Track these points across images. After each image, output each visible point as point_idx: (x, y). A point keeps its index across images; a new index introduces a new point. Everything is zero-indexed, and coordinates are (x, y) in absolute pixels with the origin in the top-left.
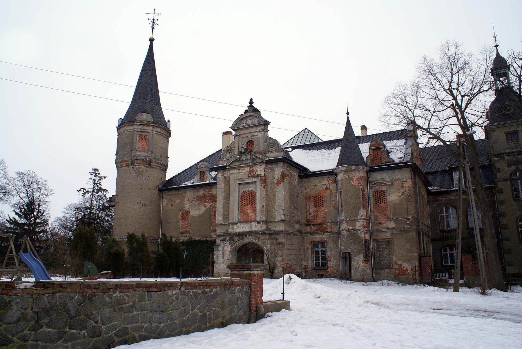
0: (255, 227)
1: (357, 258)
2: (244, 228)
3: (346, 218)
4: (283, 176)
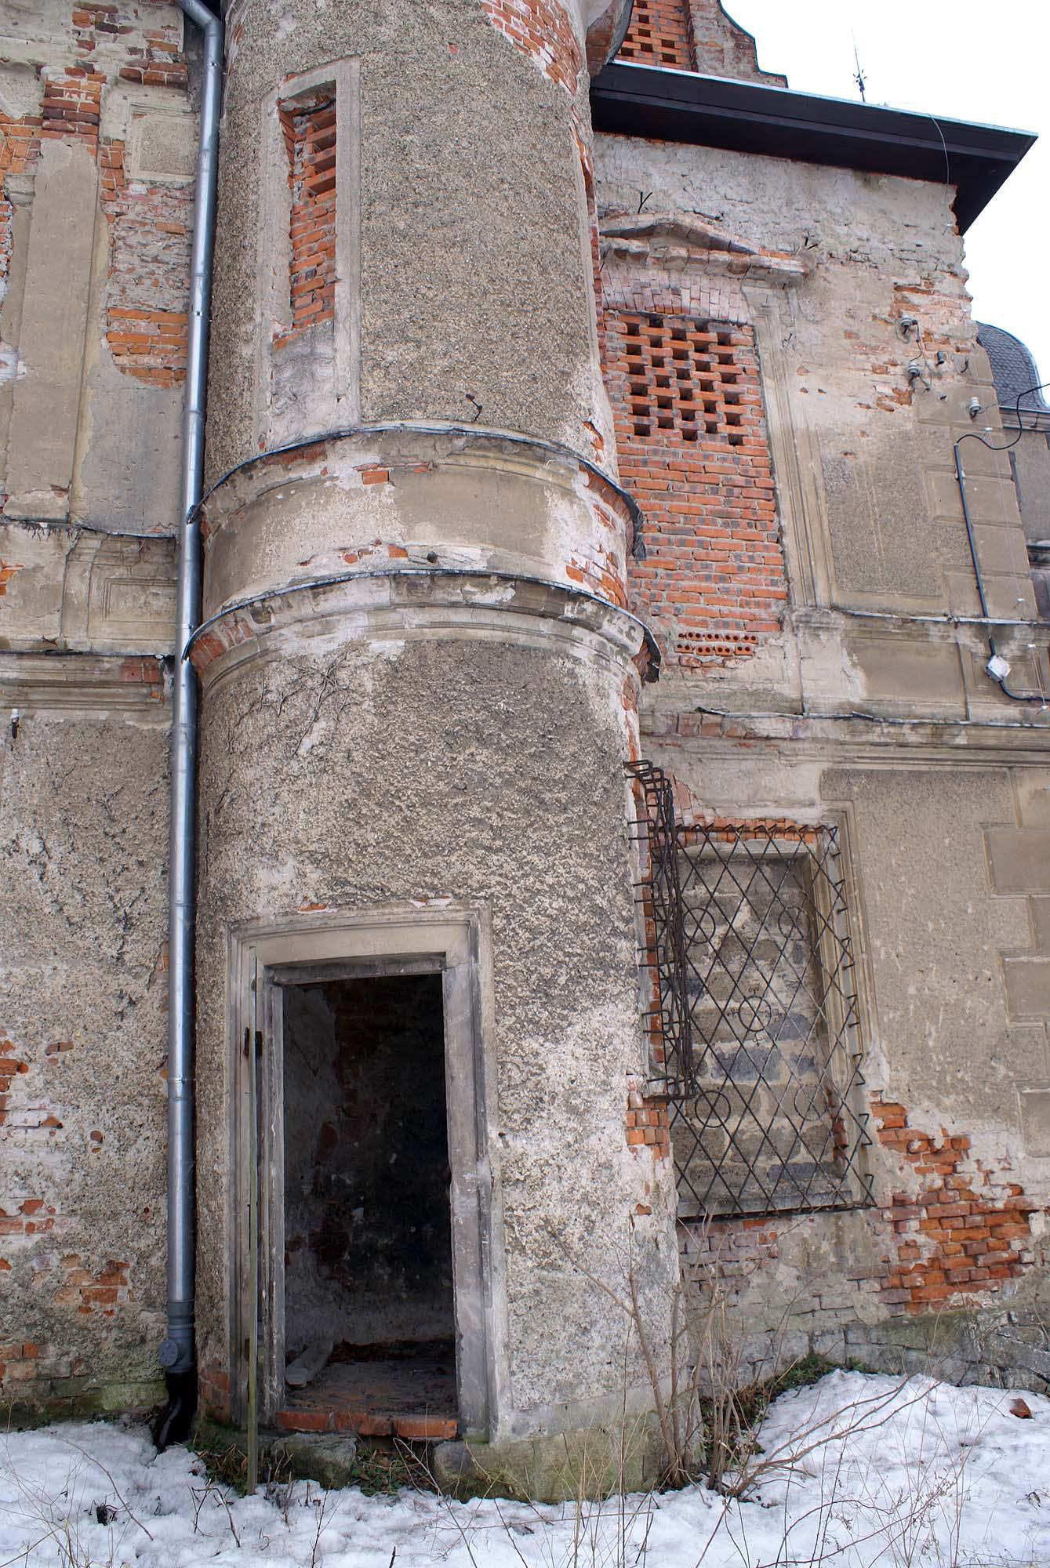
1: (562, 1062)
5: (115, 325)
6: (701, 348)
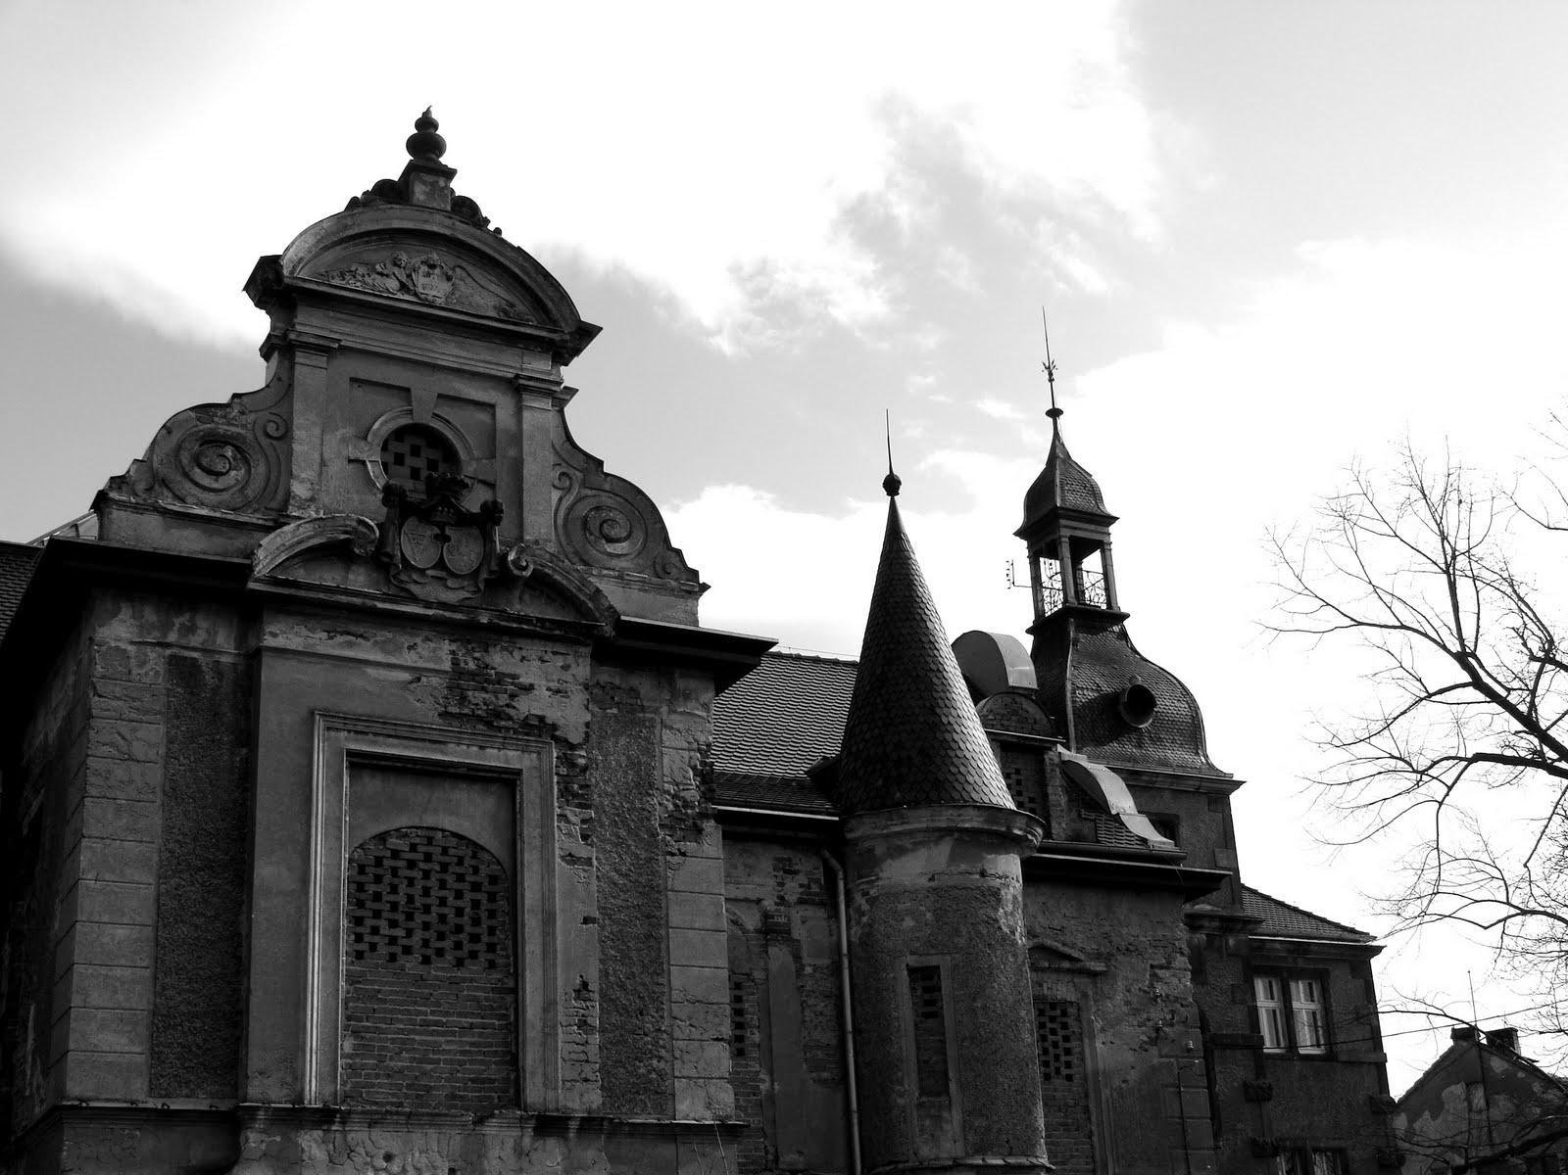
3: (981, 1150)
5: (808, 1054)
6: (1053, 1019)
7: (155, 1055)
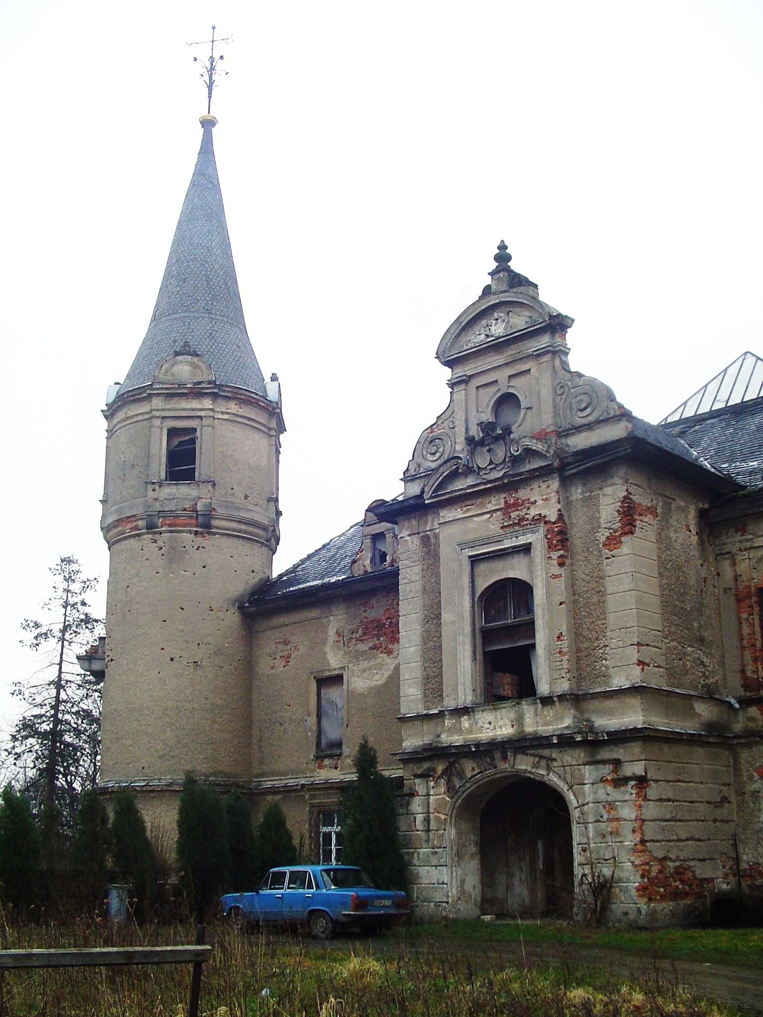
0: (536, 721)
2: (496, 725)
4: (629, 514)
7: (425, 695)
